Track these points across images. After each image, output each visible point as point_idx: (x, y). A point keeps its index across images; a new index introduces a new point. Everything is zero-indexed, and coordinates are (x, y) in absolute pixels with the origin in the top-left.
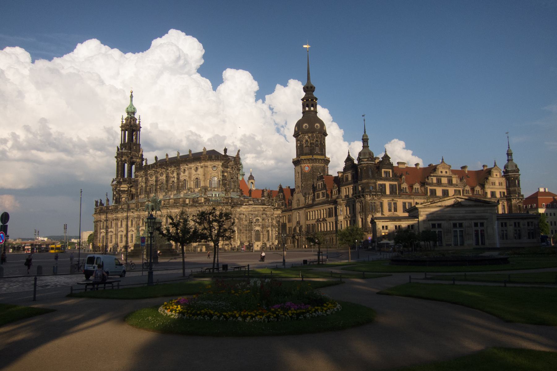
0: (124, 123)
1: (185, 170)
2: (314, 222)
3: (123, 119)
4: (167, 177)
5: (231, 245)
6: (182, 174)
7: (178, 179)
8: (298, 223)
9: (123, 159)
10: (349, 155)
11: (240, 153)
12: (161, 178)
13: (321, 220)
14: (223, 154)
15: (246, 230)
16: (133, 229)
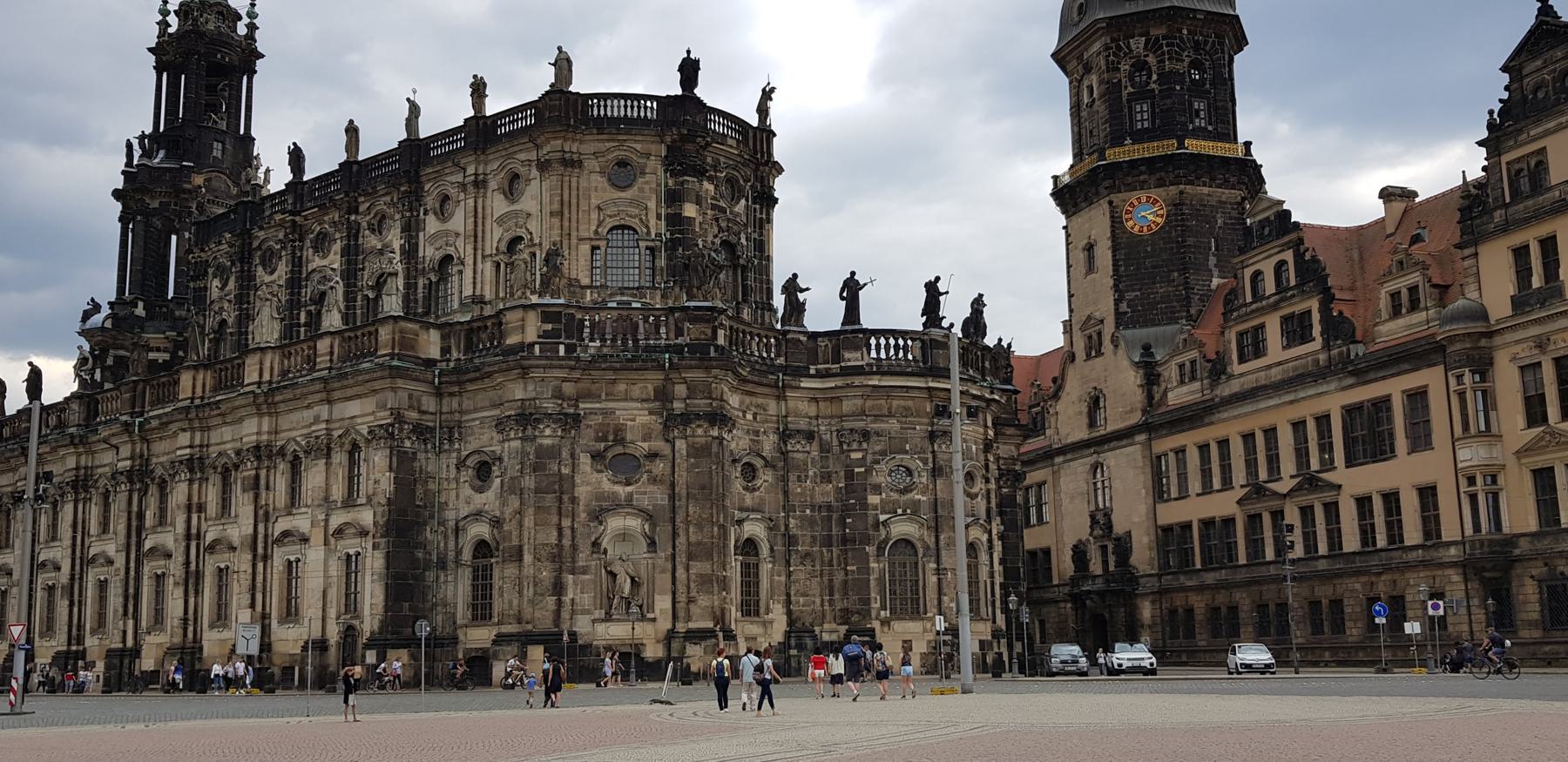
0: (171, 30)
1: (445, 199)
2: (1223, 505)
3: (164, 12)
4: (352, 253)
5: (730, 636)
6: (432, 225)
7: (410, 253)
8: (1101, 521)
9: (155, 204)
10: (1546, 10)
11: (770, 104)
12: (317, 262)
13: (1283, 486)
14: (679, 92)
15: (828, 542)
16: (111, 549)
